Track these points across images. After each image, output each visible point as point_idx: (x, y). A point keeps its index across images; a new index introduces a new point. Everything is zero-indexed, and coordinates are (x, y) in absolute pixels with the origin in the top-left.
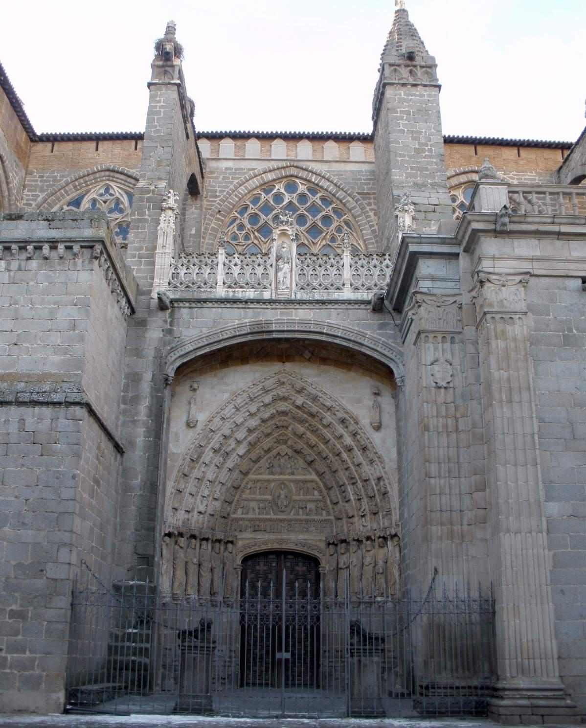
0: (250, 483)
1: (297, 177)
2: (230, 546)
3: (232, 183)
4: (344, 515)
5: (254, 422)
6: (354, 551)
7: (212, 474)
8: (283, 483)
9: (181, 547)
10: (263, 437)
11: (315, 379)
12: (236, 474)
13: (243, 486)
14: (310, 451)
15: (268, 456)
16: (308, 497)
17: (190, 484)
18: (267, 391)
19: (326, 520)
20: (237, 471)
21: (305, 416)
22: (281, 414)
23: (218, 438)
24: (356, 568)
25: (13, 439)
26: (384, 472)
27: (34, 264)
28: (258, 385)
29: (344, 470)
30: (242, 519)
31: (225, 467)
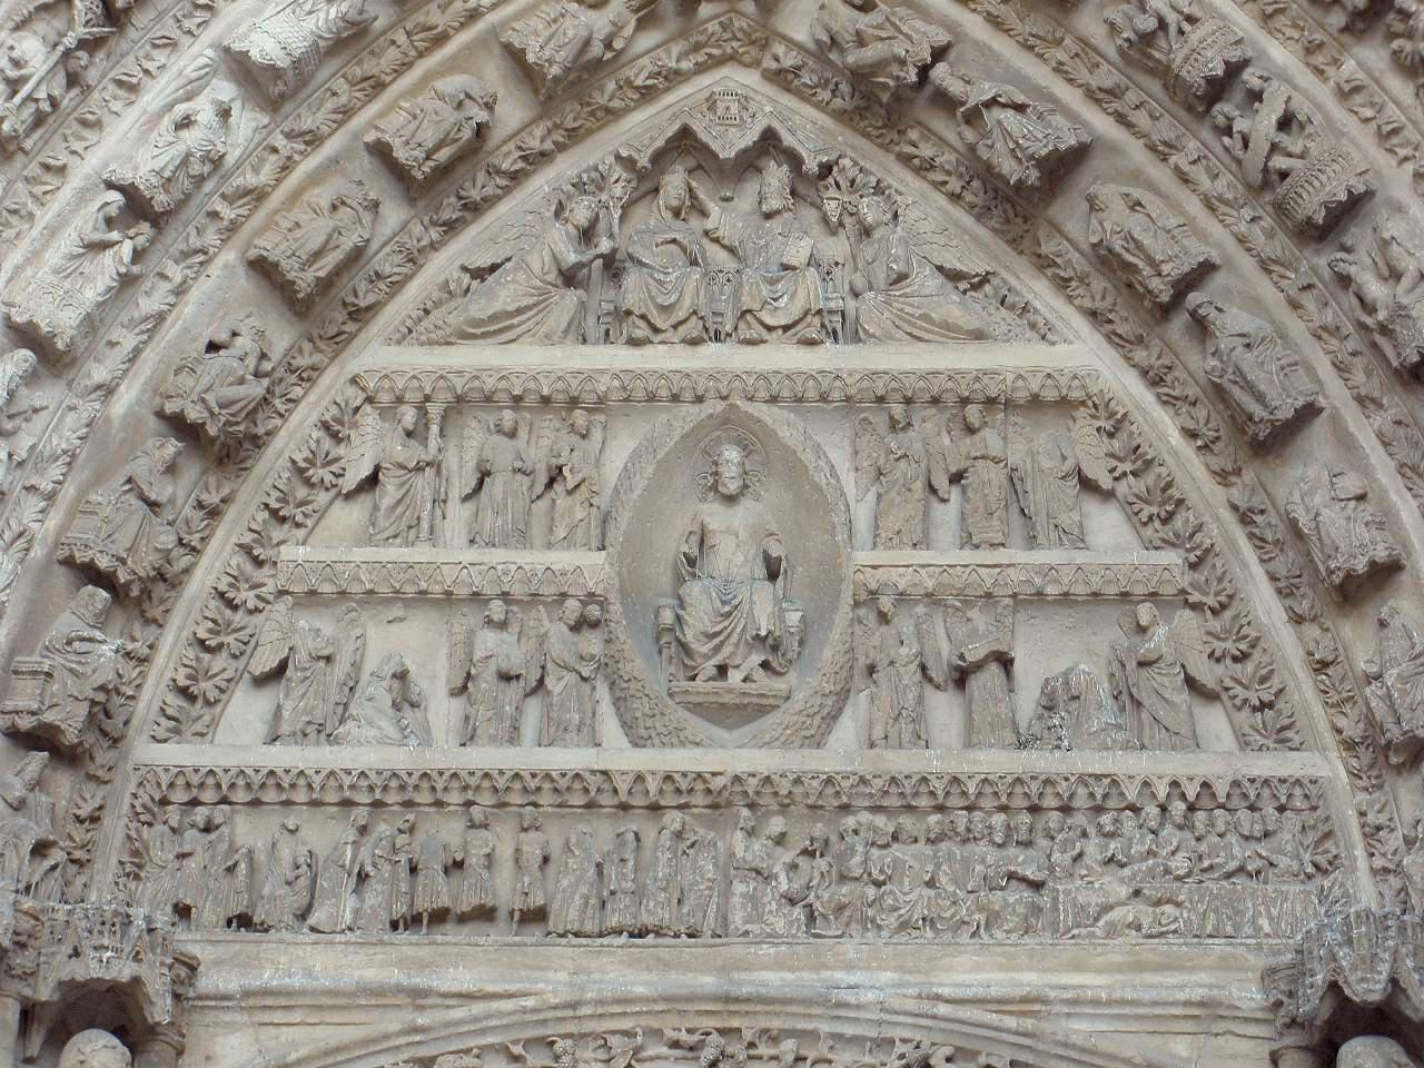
0: (369, 417)
8: (733, 425)
13: (293, 436)
14: (1041, 74)
15: (567, 167)
16: (1022, 561)
19: (1248, 795)
20: (229, 256)
31: (82, 171)
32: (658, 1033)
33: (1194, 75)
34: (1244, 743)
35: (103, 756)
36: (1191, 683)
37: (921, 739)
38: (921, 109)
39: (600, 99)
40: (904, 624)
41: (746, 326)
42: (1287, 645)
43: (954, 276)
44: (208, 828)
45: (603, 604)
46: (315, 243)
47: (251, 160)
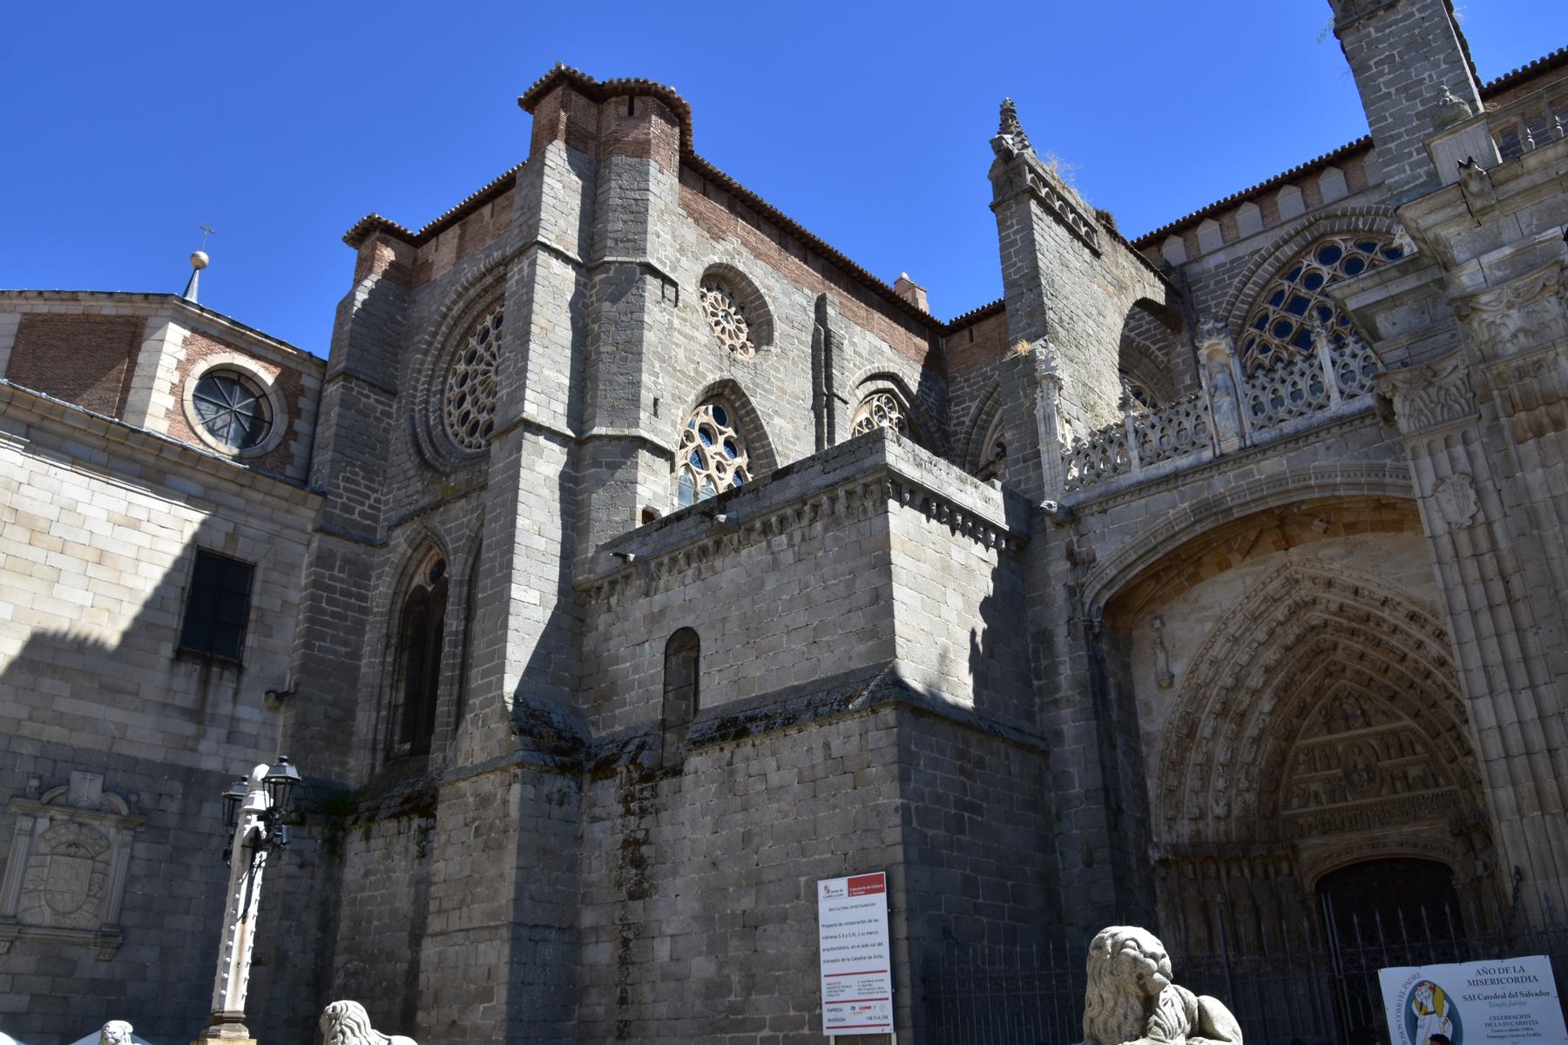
1: (1333, 233)
3: (1230, 285)
5: (1270, 656)
11: (1344, 562)
15: (1320, 703)
23: (1218, 694)
25: (820, 774)
27: (818, 526)
30: (1300, 815)
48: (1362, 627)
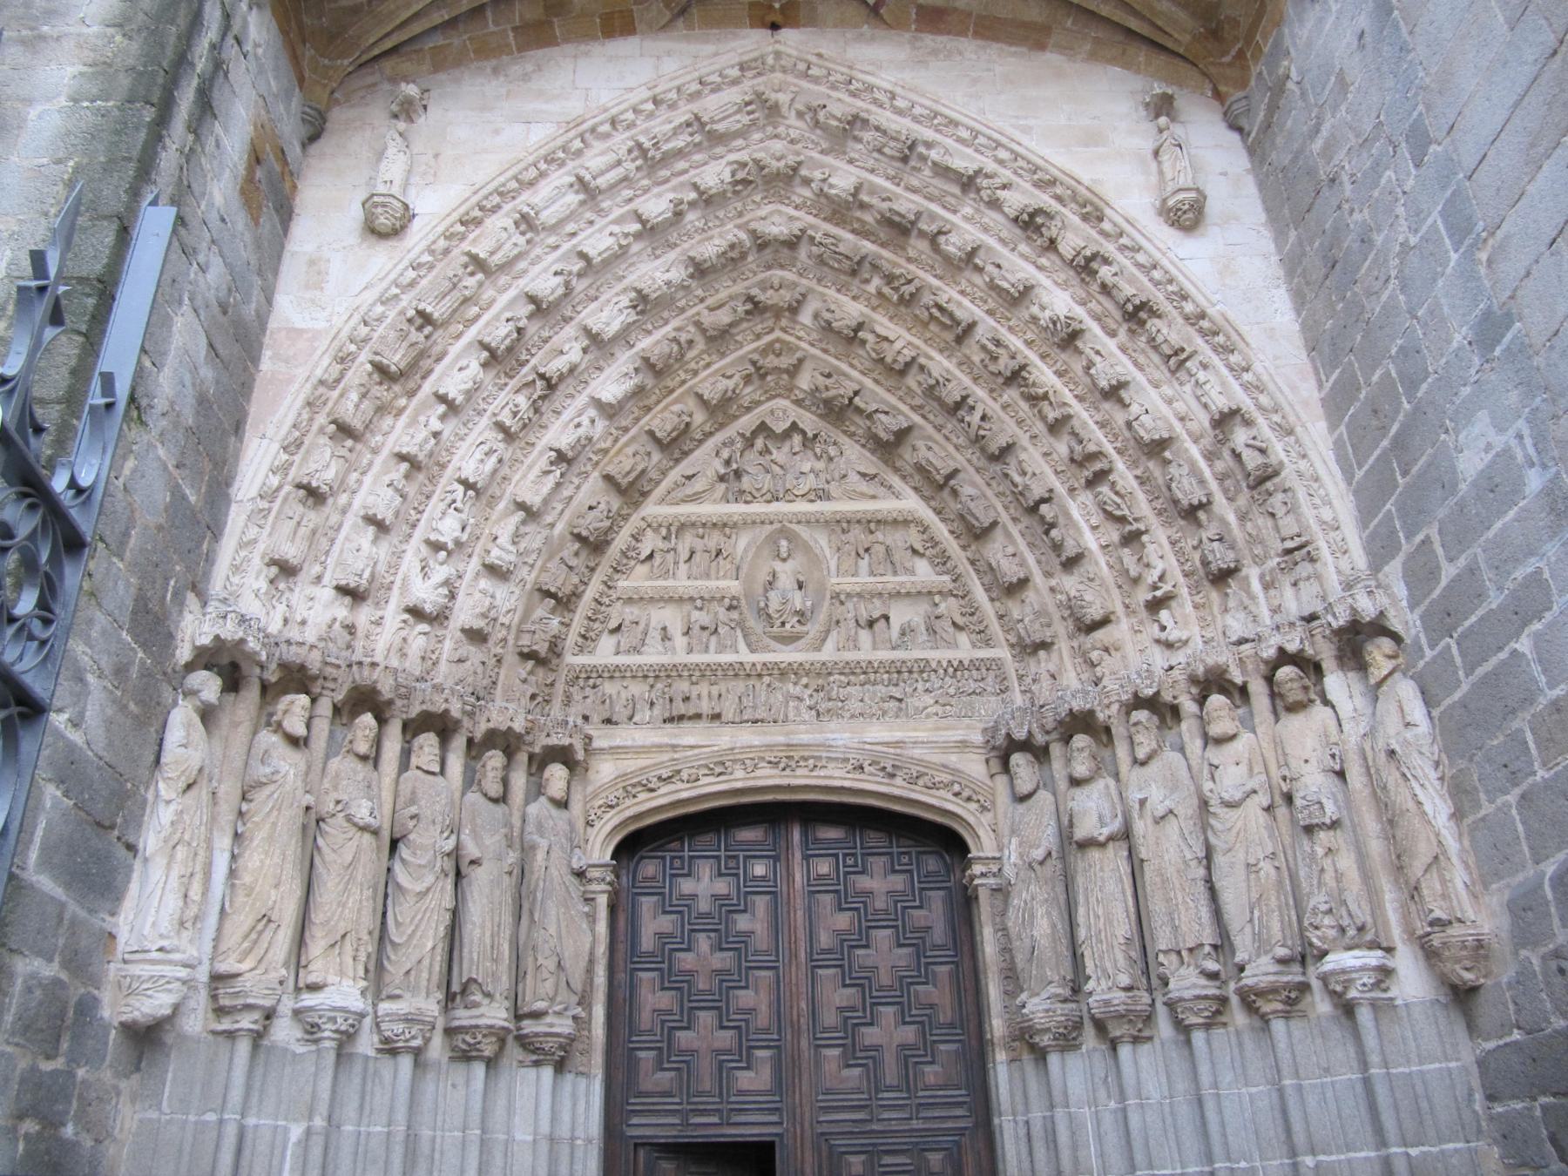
0: (649, 532)
2: (557, 774)
4: (1060, 629)
6: (1141, 754)
7: (478, 456)
8: (784, 533)
9: (294, 741)
10: (700, 345)
11: (907, 76)
12: (589, 490)
13: (621, 540)
14: (893, 400)
15: (719, 437)
16: (891, 581)
17: (368, 479)
18: (712, 138)
19: (975, 665)
20: (596, 474)
21: (868, 246)
22: (768, 254)
24: (1172, 827)
26: (1246, 387)
28: (673, 106)
29: (1047, 440)
30: (614, 673)
31: (541, 445)
32: (763, 759)
33: (950, 401)
34: (974, 646)
35: (555, 661)
36: (954, 624)
37: (857, 648)
38: (850, 413)
39: (731, 412)
40: (850, 605)
41: (788, 495)
42: (988, 609)
43: (863, 475)
44: (594, 687)
45: (738, 600)
46: (627, 468)
47: (603, 438)
48: (885, 253)
